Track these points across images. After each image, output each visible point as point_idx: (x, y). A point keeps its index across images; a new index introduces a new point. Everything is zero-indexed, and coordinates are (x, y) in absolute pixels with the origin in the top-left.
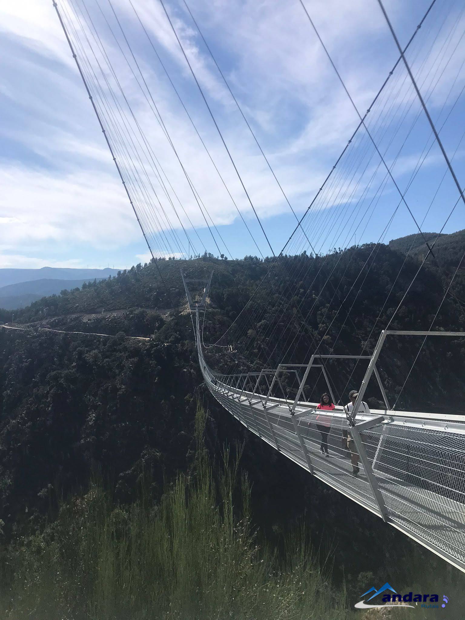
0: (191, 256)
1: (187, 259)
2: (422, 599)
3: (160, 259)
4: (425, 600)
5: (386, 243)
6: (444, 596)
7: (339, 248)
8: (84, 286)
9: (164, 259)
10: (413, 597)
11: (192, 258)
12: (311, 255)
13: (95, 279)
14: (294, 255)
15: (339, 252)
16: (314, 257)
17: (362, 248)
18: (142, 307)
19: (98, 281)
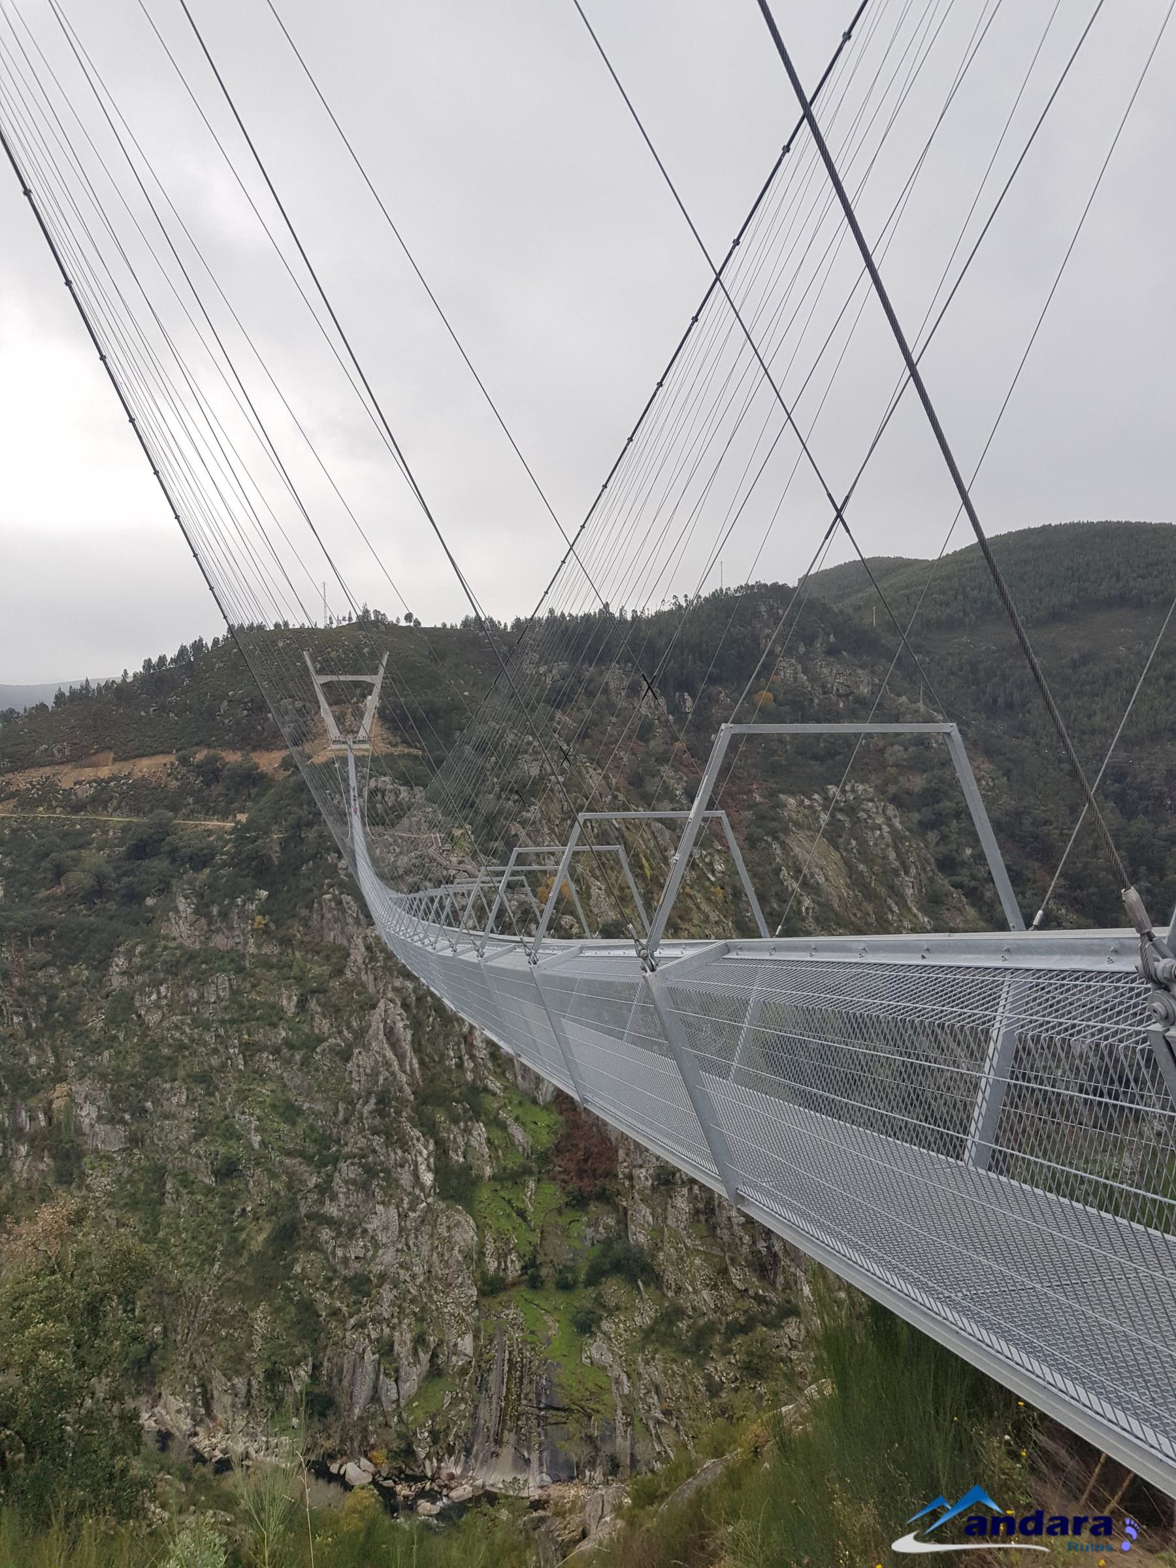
0: (330, 618)
1: (321, 626)
3: (251, 627)
5: (793, 583)
7: (686, 596)
8: (60, 697)
9: (261, 627)
11: (332, 623)
12: (621, 614)
13: (87, 681)
14: (581, 614)
15: (684, 605)
16: (629, 617)
17: (738, 594)
18: (209, 746)
19: (94, 686)
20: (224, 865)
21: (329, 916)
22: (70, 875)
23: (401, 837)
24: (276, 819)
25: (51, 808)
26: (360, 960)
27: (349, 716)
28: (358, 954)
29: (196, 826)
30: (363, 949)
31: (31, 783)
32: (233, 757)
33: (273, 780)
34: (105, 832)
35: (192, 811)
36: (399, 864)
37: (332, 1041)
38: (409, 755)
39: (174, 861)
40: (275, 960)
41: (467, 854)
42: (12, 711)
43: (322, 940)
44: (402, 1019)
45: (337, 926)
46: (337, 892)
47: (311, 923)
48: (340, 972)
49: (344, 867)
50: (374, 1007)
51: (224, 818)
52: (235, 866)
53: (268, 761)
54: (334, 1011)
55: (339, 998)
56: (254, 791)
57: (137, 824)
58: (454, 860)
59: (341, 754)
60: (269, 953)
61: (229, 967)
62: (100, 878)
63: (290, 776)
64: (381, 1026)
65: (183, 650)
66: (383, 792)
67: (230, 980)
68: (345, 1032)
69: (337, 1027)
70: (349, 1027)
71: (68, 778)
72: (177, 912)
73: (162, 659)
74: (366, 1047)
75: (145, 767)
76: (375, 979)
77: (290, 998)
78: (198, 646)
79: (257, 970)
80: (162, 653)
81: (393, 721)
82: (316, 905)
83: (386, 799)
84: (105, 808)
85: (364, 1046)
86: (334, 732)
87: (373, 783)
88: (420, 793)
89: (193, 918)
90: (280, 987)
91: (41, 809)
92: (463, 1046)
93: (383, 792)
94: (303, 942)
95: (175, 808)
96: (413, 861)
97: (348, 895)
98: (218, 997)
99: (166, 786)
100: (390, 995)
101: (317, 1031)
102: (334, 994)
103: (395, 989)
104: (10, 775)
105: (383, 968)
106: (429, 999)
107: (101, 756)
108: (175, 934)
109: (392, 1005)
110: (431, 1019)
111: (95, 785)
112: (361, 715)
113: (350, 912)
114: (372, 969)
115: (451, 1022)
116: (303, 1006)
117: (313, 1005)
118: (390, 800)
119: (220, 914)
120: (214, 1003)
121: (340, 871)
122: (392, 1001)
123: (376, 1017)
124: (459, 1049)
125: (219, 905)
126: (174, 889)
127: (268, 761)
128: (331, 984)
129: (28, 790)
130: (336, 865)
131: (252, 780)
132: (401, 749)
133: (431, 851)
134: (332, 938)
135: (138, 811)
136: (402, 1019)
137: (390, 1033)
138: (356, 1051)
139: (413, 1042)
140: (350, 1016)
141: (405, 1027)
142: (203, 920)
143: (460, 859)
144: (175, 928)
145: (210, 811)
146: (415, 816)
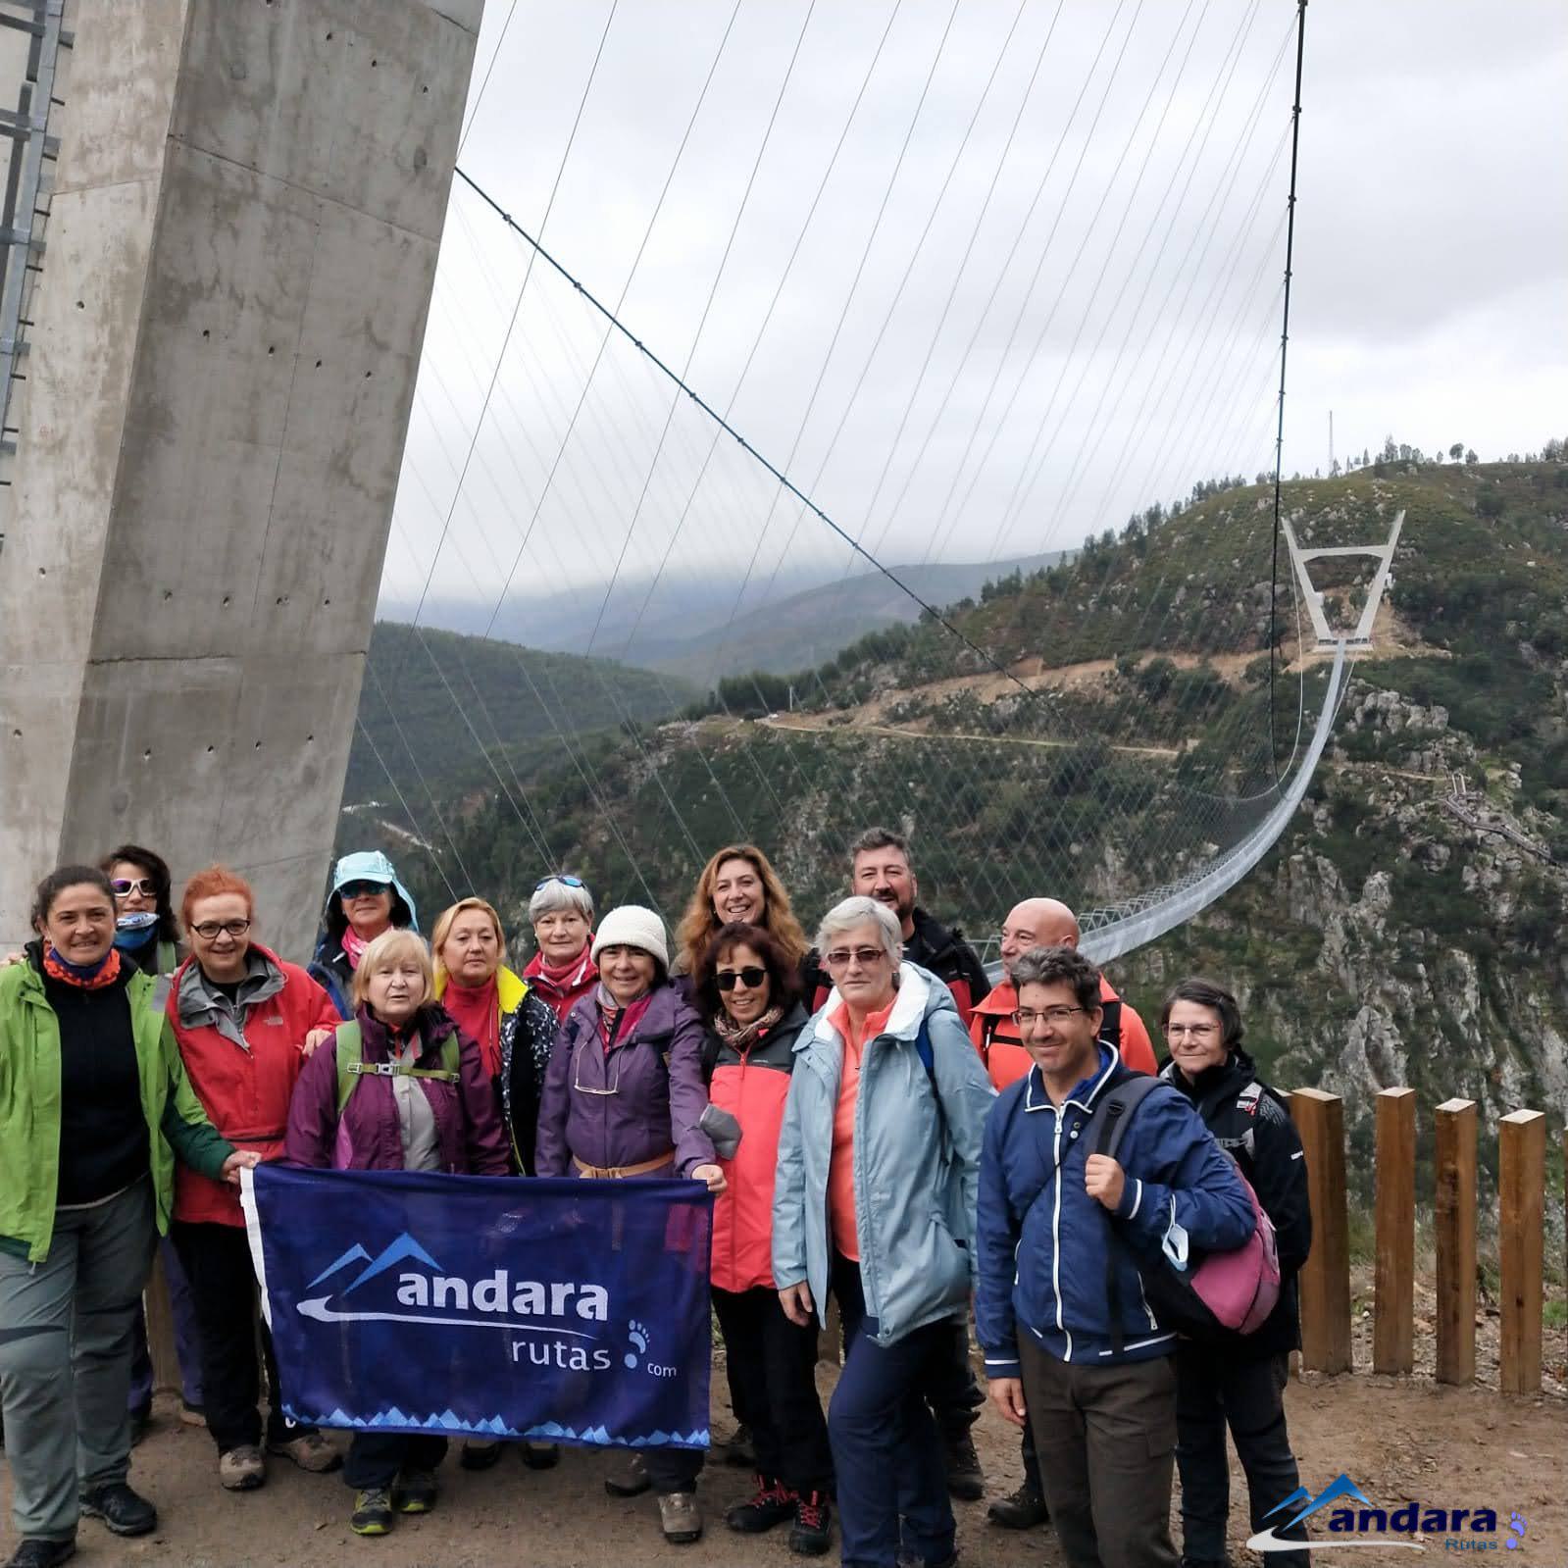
2: (1449, 1521)
4: (1456, 1527)
6: (632, 1325)
8: (988, 593)
10: (1421, 1518)
18: (1158, 648)
19: (1025, 574)
20: (1165, 807)
21: (1298, 884)
22: (986, 810)
23: (1407, 779)
24: (1233, 748)
25: (968, 729)
26: (1338, 949)
27: (1347, 603)
28: (1335, 940)
29: (1137, 754)
30: (1341, 934)
31: (948, 697)
32: (1185, 663)
33: (1238, 695)
34: (1027, 759)
35: (1133, 734)
36: (1400, 817)
37: (1296, 1054)
38: (1432, 658)
39: (1103, 800)
40: (1223, 938)
41: (1507, 807)
42: (935, 608)
43: (1288, 917)
44: (1393, 1037)
45: (1310, 899)
46: (1310, 853)
47: (1273, 893)
48: (1308, 961)
49: (1322, 817)
50: (1353, 1015)
51: (1172, 745)
52: (1177, 808)
53: (1231, 668)
54: (1299, 1013)
55: (1307, 998)
56: (1213, 709)
57: (1068, 751)
58: (1484, 814)
59: (1326, 658)
60: (1217, 927)
61: (1165, 942)
62: (1020, 818)
63: (1256, 690)
64: (1363, 1042)
65: (1133, 527)
66: (1385, 714)
67: (1165, 958)
68: (1314, 1045)
69: (1304, 1036)
70: (1320, 1038)
71: (996, 692)
72: (1104, 864)
73: (1108, 536)
74: (1341, 1070)
75: (1080, 677)
76: (1358, 978)
77: (1241, 989)
78: (1154, 516)
79: (1201, 949)
80: (1107, 528)
81: (1412, 608)
82: (1281, 868)
83: (1389, 723)
84: (1030, 729)
85: (1337, 1068)
86: (1322, 629)
87: (1370, 702)
88: (1439, 717)
89: (1121, 874)
90: (1229, 976)
91: (958, 729)
92: (1484, 1085)
93: (1385, 714)
94: (1261, 917)
95: (1112, 730)
96: (1423, 814)
97: (1325, 857)
98: (1151, 978)
99: (1102, 702)
100: (1378, 1001)
101: (1277, 1039)
102: (1299, 993)
103: (1385, 994)
104: (926, 688)
105: (1371, 962)
106: (1435, 1013)
107: (1028, 663)
108: (1100, 892)
109: (1378, 1016)
110: (1437, 1042)
111: (1019, 699)
112: (1359, 601)
113: (1327, 881)
114: (1354, 962)
115: (1468, 1049)
116: (1260, 1002)
117: (1272, 1001)
118: (1394, 725)
119: (1157, 871)
120: (1146, 985)
121: (1317, 824)
122: (1379, 1009)
123: (1355, 1030)
124: (1478, 1090)
125: (1158, 858)
126: (1103, 835)
127: (1231, 668)
128: (1297, 978)
129: (945, 705)
130: (1312, 815)
131: (1207, 692)
132: (1424, 650)
133: (1451, 803)
134: (1301, 916)
135: (1065, 732)
136: (1393, 1037)
137: (1375, 1053)
138: (1326, 1072)
139: (1407, 1070)
140: (1321, 1023)
141: (1397, 1048)
142: (1135, 879)
143: (1494, 814)
144: (1101, 884)
145: (1155, 735)
146: (1429, 749)
